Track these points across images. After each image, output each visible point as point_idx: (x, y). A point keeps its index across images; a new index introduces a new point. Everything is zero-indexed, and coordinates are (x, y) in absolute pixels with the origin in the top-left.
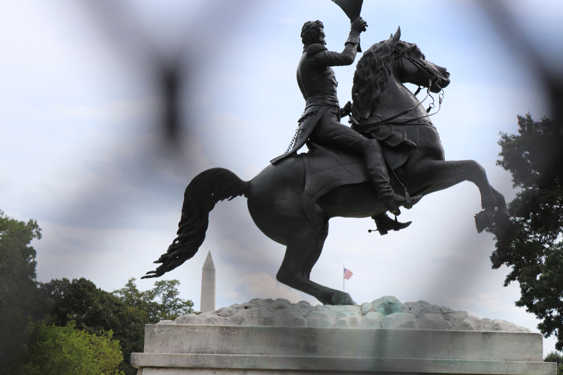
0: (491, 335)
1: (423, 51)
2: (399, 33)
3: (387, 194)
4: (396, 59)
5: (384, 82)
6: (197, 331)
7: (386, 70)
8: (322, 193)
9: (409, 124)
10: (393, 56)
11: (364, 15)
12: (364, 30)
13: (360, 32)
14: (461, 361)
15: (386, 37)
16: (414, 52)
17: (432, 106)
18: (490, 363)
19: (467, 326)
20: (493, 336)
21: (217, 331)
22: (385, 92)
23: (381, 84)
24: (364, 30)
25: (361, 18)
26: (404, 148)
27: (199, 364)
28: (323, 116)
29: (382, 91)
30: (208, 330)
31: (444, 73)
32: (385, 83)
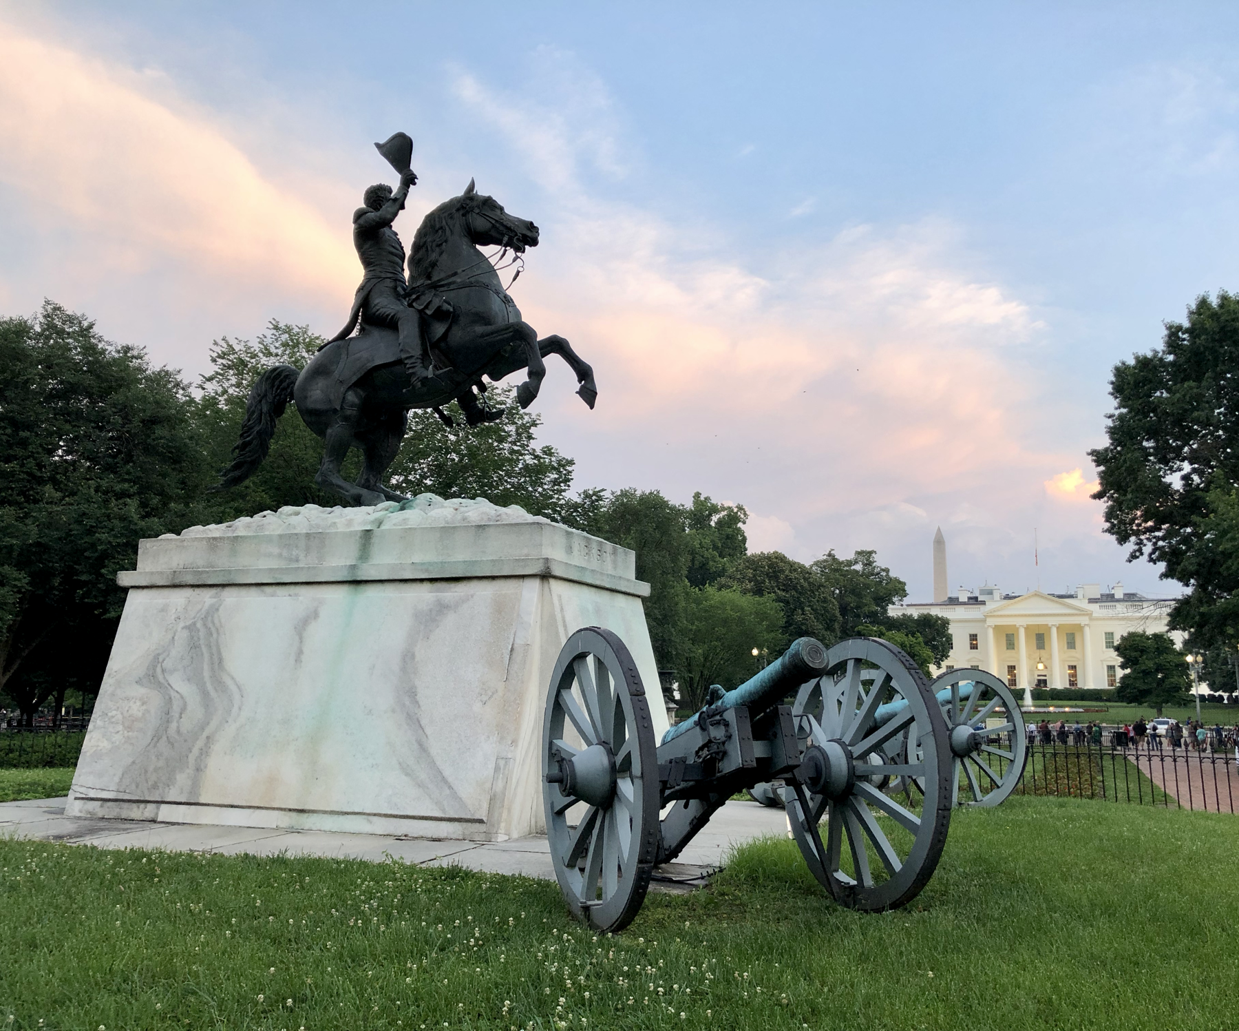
0: (484, 529)
1: (500, 202)
2: (472, 187)
3: (411, 371)
4: (463, 215)
5: (442, 244)
6: (185, 544)
7: (447, 229)
8: (355, 379)
9: (442, 283)
10: (462, 212)
11: (415, 166)
12: (415, 184)
13: (409, 187)
14: (442, 562)
15: (460, 192)
16: (489, 203)
17: (521, 269)
18: (473, 563)
19: (464, 519)
20: (487, 529)
21: (205, 543)
22: (444, 256)
23: (439, 245)
24: (415, 184)
25: (410, 170)
26: (440, 315)
27: (177, 581)
28: (370, 291)
29: (441, 254)
30: (196, 543)
31: (531, 227)
32: (444, 244)
